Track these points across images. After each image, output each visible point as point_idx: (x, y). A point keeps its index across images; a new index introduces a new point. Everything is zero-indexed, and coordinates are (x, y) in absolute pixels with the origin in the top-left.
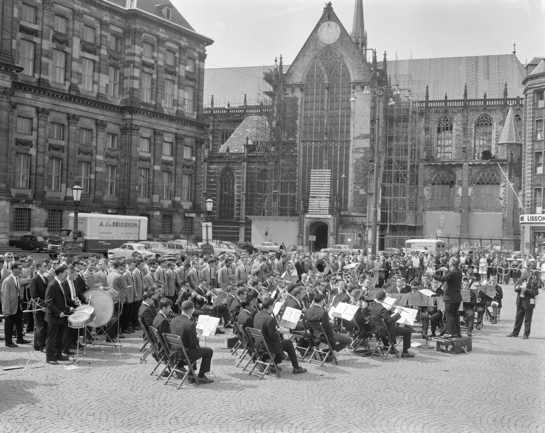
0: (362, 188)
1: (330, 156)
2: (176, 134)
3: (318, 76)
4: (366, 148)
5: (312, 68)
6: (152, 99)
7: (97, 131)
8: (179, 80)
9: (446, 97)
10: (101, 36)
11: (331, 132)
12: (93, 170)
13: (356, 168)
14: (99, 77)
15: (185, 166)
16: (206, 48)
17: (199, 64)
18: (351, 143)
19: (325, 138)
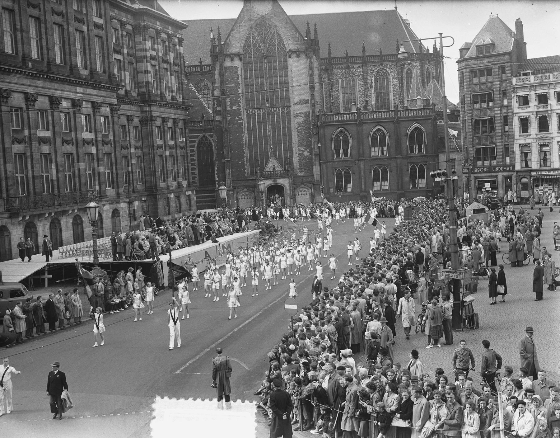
0: (306, 150)
1: (273, 121)
2: (174, 119)
3: (255, 46)
4: (306, 113)
5: (248, 38)
6: (157, 89)
7: (129, 126)
8: (170, 67)
9: (347, 54)
10: (122, 35)
11: (272, 99)
12: (130, 163)
13: (299, 132)
14: (125, 75)
15: (181, 148)
16: (183, 32)
17: (180, 49)
18: (292, 109)
19: (268, 105)
